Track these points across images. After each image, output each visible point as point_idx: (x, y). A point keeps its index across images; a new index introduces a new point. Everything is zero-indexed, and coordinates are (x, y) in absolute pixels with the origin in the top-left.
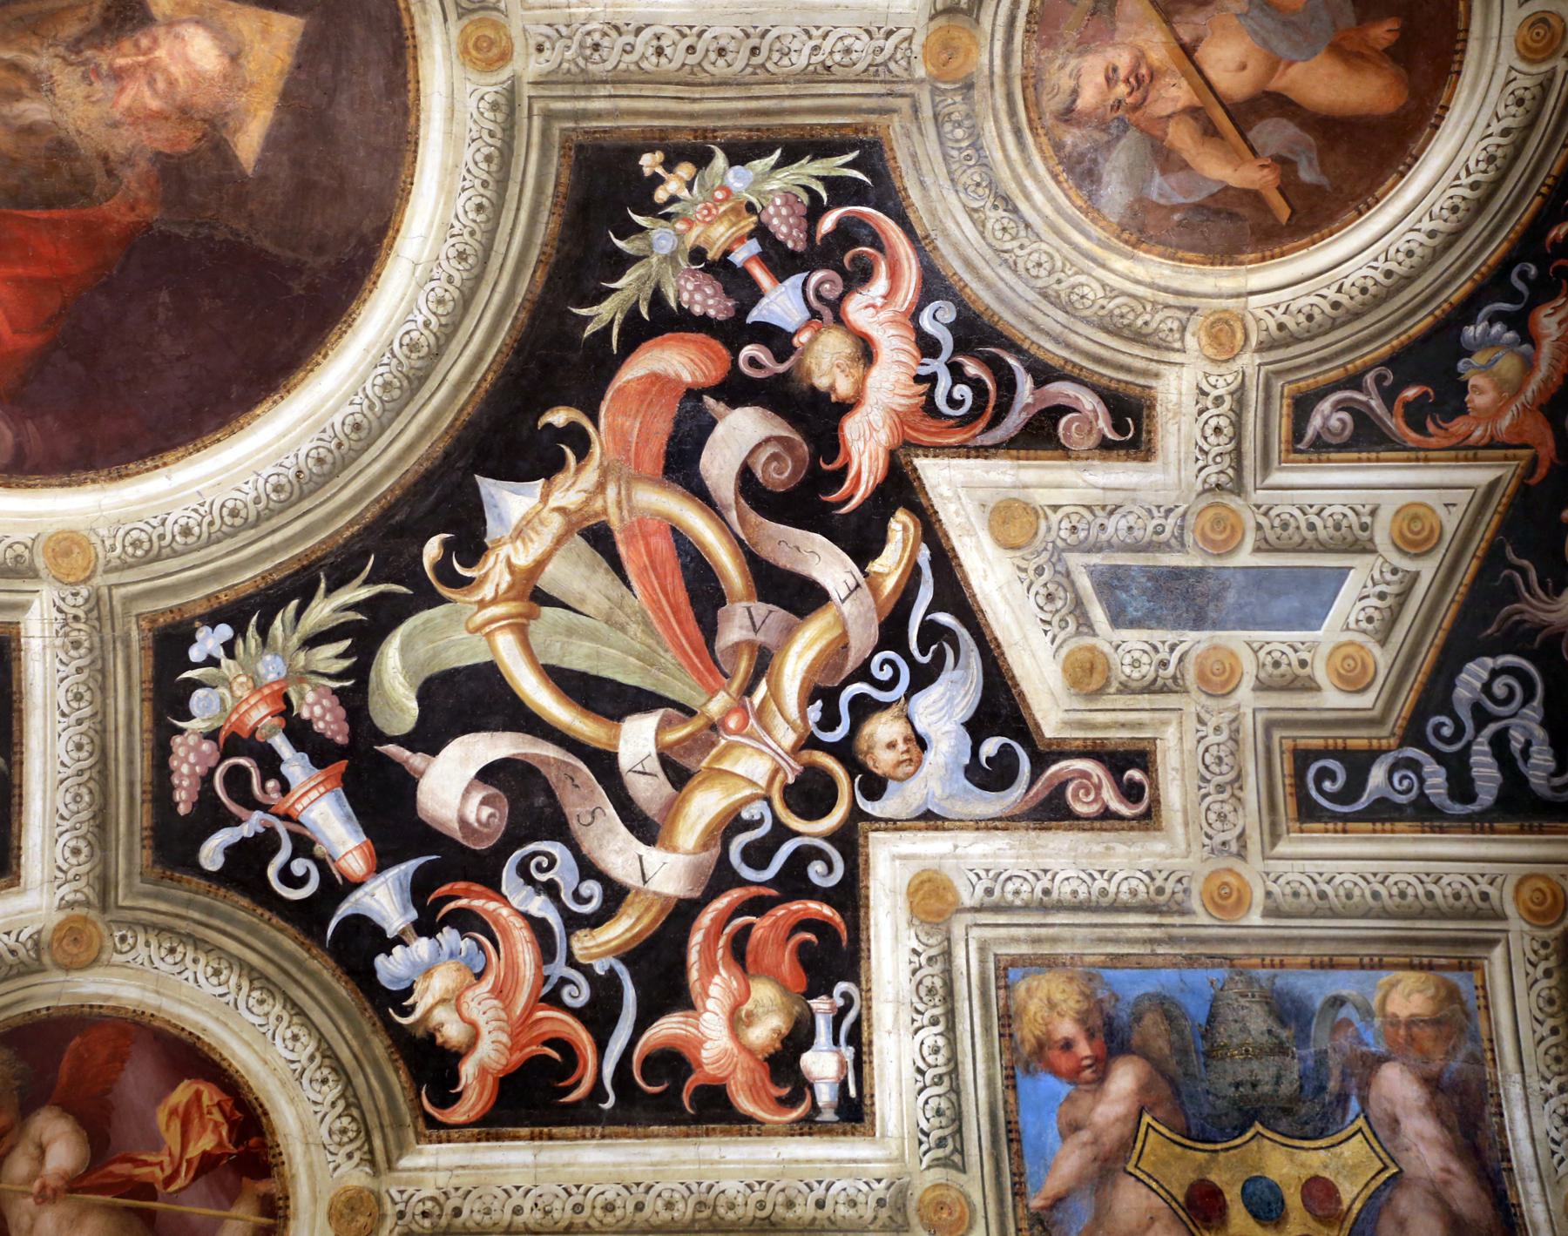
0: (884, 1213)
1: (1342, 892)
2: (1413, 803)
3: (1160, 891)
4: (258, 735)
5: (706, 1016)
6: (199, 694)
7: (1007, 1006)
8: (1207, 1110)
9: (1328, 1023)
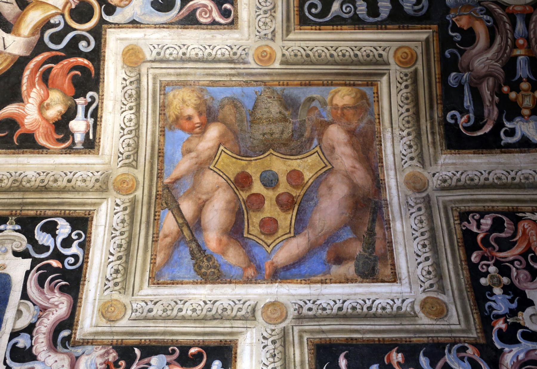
0: (98, 185)
1: (316, 54)
2: (351, 18)
3: (235, 54)
5: (28, 105)
7: (164, 102)
8: (249, 144)
9: (306, 108)
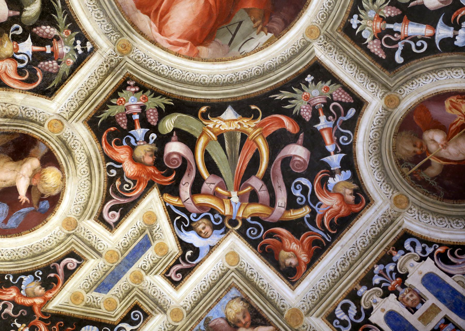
4: (383, 29)
6: (363, 33)
